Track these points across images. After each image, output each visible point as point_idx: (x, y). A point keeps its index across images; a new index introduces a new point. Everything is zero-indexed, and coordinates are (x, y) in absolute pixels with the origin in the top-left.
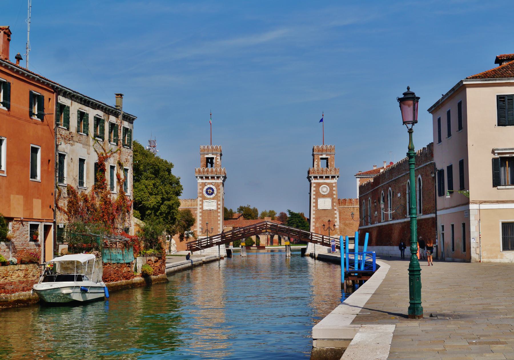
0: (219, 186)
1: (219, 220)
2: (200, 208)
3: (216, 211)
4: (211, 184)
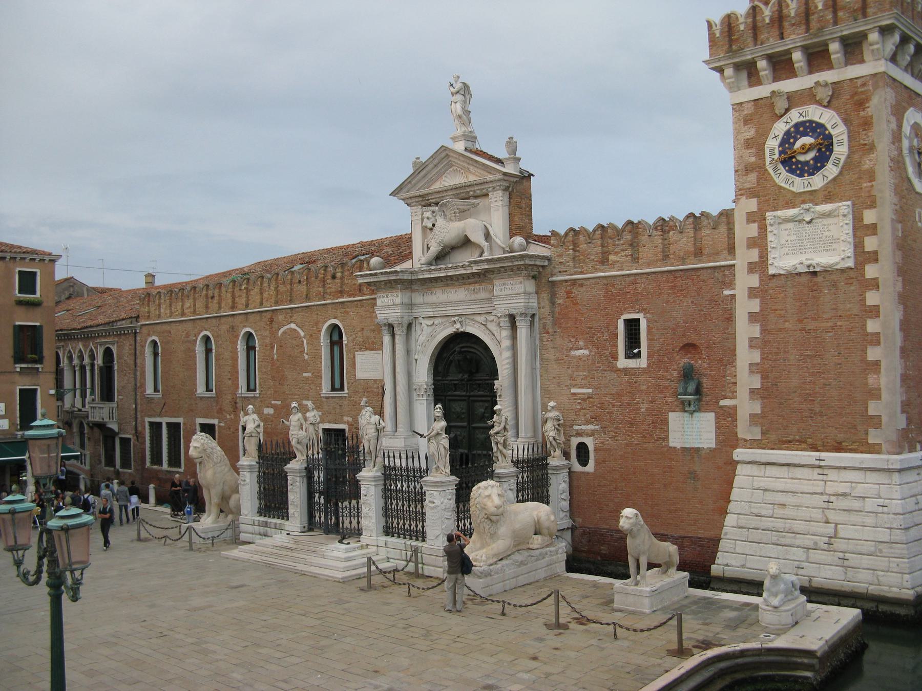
0: (861, 104)
1: (875, 340)
2: (752, 268)
3: (854, 277)
4: (808, 97)
